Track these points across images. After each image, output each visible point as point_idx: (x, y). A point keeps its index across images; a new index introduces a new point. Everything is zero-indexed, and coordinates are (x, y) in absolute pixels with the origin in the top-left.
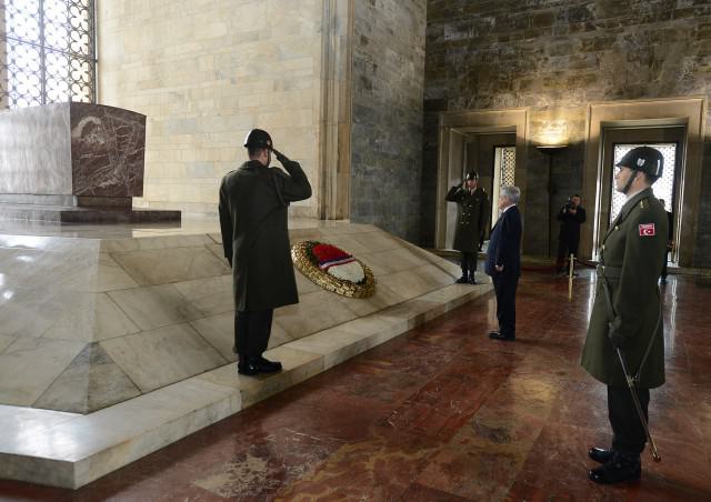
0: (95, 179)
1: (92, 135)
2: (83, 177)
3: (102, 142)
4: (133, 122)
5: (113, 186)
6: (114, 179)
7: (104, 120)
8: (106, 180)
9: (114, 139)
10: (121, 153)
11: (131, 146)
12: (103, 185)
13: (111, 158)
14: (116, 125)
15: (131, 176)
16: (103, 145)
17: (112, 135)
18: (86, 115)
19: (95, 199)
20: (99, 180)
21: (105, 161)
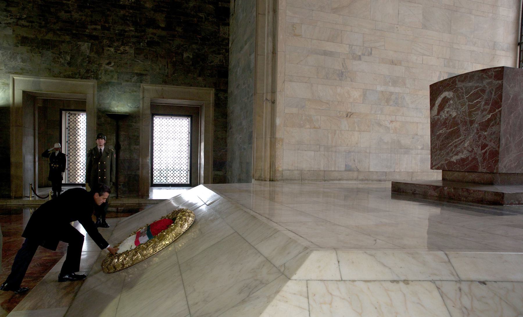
0: (448, 154)
1: (446, 110)
2: (438, 152)
3: (454, 114)
4: (485, 83)
5: (463, 160)
6: (465, 152)
7: (456, 91)
8: (457, 154)
9: (465, 108)
10: (472, 122)
11: (484, 110)
12: (454, 159)
13: (462, 129)
14: (467, 92)
15: (484, 146)
16: (455, 118)
17: (463, 105)
18: (441, 92)
19: (456, 174)
20: (451, 155)
21: (455, 133)
